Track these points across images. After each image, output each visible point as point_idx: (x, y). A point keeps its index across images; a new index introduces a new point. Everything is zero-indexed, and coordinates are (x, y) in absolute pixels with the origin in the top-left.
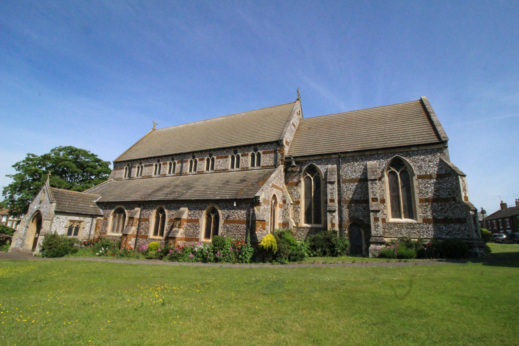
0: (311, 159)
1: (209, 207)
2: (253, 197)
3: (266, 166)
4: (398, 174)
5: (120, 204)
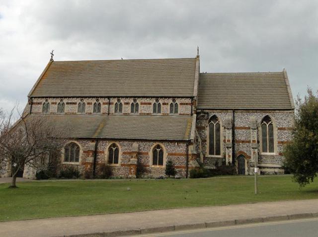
0: (215, 111)
1: (155, 144)
3: (183, 114)
4: (268, 125)
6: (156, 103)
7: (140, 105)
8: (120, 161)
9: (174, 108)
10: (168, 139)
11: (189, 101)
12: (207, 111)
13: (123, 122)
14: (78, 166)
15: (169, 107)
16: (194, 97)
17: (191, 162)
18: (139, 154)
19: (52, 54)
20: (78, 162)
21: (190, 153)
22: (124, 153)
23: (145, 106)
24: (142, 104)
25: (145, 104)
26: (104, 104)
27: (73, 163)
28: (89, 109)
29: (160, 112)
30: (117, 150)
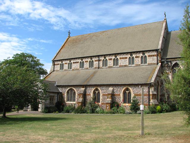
2: (150, 83)
3: (151, 64)
5: (71, 87)
6: (131, 57)
7: (119, 60)
8: (101, 101)
9: (144, 60)
10: (133, 83)
11: (156, 53)
12: (169, 60)
13: (109, 73)
14: (75, 104)
15: (140, 59)
16: (158, 49)
17: (152, 101)
18: (113, 95)
19: (69, 33)
20: (75, 101)
21: (151, 93)
22: (103, 95)
23: (123, 60)
24: (120, 58)
25: (123, 58)
26: (95, 61)
27: (72, 102)
28: (86, 65)
29: (134, 64)
30: (99, 93)
